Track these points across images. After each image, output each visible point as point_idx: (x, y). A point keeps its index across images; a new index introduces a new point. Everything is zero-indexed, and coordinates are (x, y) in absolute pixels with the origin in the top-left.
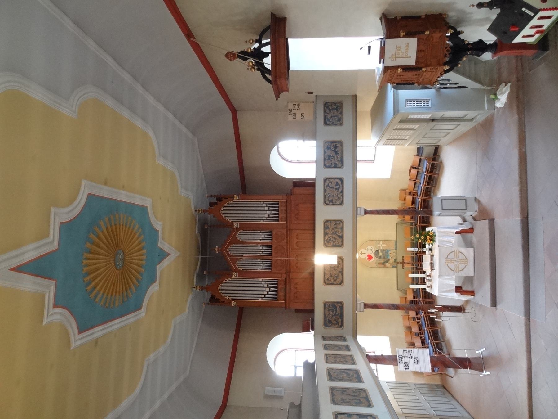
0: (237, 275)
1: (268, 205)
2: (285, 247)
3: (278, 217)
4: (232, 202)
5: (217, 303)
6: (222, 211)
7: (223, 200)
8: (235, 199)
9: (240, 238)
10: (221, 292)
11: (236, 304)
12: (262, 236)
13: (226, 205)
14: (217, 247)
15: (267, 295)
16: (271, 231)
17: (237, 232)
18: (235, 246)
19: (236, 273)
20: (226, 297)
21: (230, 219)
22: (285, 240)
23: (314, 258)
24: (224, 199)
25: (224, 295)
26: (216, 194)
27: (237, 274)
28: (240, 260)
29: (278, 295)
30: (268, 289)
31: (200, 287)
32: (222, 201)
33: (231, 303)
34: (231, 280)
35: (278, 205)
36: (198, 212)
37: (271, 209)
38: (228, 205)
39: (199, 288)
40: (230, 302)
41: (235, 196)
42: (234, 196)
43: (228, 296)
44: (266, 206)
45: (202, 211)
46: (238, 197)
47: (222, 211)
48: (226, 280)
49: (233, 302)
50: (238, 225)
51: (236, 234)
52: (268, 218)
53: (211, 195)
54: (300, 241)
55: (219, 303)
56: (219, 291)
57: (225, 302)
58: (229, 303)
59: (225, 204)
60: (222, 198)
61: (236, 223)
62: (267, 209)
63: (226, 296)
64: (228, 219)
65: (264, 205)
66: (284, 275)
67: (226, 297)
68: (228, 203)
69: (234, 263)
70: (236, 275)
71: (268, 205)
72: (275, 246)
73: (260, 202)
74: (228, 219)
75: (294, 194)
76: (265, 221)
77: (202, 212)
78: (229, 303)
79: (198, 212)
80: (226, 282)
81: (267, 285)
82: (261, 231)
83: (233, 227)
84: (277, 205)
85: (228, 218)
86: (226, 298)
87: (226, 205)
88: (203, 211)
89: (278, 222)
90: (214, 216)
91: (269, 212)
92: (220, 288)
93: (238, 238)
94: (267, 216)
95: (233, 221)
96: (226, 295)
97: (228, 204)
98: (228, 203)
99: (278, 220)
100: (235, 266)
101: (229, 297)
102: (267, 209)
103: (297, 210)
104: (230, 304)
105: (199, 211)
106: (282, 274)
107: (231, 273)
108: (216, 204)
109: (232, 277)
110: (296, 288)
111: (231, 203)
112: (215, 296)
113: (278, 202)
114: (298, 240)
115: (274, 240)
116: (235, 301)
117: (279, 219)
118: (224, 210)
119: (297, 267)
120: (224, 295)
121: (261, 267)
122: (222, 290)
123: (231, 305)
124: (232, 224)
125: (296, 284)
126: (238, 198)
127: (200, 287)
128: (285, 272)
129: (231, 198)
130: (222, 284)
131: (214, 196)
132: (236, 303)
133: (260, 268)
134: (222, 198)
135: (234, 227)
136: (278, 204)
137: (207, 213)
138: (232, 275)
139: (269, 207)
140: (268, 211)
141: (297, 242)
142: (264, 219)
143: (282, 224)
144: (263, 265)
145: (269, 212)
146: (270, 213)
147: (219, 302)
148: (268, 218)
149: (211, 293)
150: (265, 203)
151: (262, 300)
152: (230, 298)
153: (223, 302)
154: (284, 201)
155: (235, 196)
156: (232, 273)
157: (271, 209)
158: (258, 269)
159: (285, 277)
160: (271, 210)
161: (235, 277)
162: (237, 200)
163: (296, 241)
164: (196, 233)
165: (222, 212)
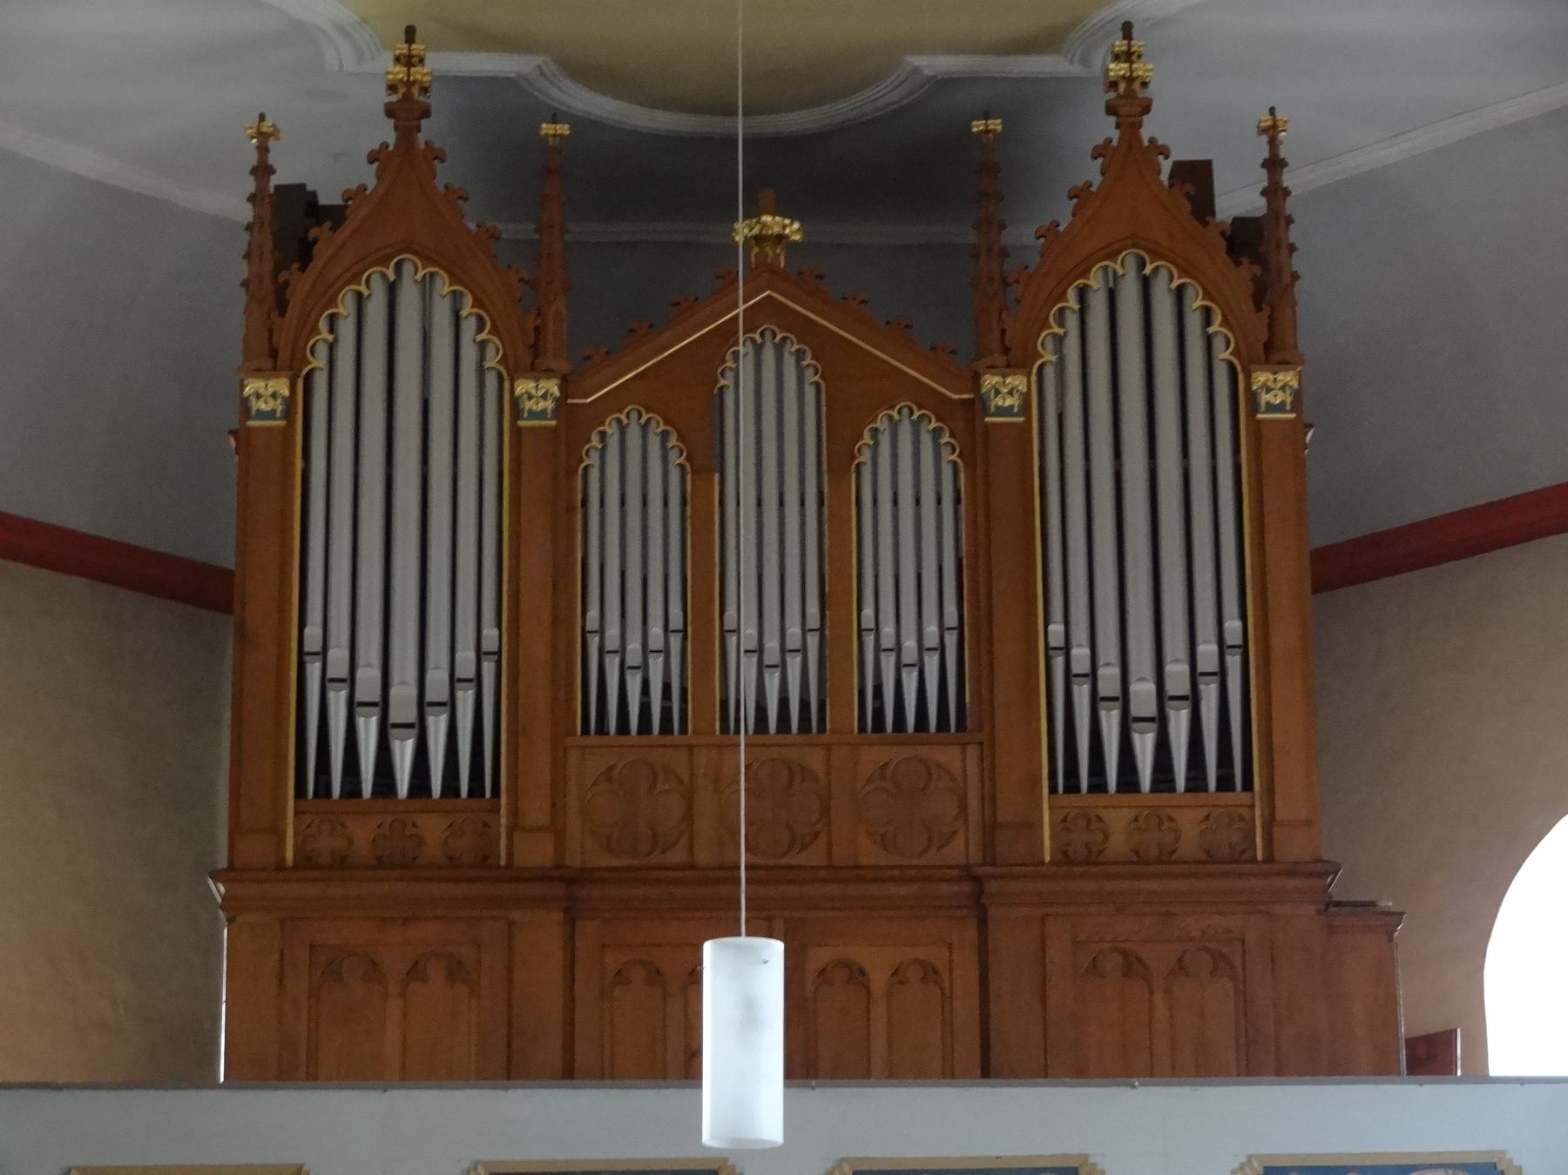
0: (534, 415)
1: (1209, 692)
2: (814, 856)
3: (1098, 785)
4: (1222, 354)
5: (269, 246)
6: (1142, 265)
7: (1247, 270)
8: (1261, 377)
9: (885, 440)
10: (377, 283)
11: (262, 415)
12: (910, 644)
13: (1195, 301)
14: (793, 229)
15: (352, 705)
16: (961, 726)
17: (942, 408)
18: (810, 392)
19: (549, 405)
20: (323, 325)
21: (1059, 340)
22: (871, 855)
23: (748, 934)
24: (1254, 279)
25: (345, 307)
26: (1290, 206)
27: (542, 415)
28: (673, 441)
29: (351, 804)
30: (403, 707)
31: (415, 90)
32: (1238, 264)
33: (274, 370)
34: (481, 371)
35: (1220, 788)
36: (1120, 45)
37: (1179, 722)
38: (1194, 322)
39: (409, 84)
40: (284, 355)
41: (1288, 377)
42: (1285, 364)
43: (332, 347)
44: (1201, 668)
45: (1130, 79)
46: (1280, 407)
47: (1142, 265)
48: (480, 329)
49: (282, 386)
50: (1007, 411)
51: (924, 397)
52: (1082, 693)
53: (1283, 164)
54: (879, 1011)
55: (267, 266)
56: (384, 261)
57: (282, 314)
58: (274, 354)
59: (1208, 295)
60: (1258, 259)
61: (1026, 398)
62: (1177, 673)
63: (332, 330)
64: (1061, 324)
65: (1213, 648)
66: (536, 852)
67: (323, 325)
68: (1218, 318)
69: (647, 394)
70: (529, 405)
71: (1209, 692)
72: (815, 760)
73: (1243, 617)
74: (1061, 324)
75: (1331, 930)
76: (1059, 662)
77: (1122, 87)
78: (274, 354)
79: (1120, 45)
80: (469, 327)
81: (444, 696)
82: (960, 628)
83: (992, 368)
84: (1219, 779)
85: (1072, 321)
86: (315, 330)
87: (1199, 303)
88: (1130, 95)
89: (1053, 789)
90: (1081, 195)
91: (1143, 692)
92: (407, 269)
93: (882, 424)
94: (1109, 676)
95: (1050, 373)
96: (347, 328)
97: (1208, 322)
98: (1218, 318)
99: (1072, 787)
100: (614, 402)
101: (322, 351)
102: (1177, 673)
103: (1181, 967)
104: (268, 363)
105: (1128, 56)
106: (557, 829)
107: (554, 365)
108: (1203, 204)
109: (514, 368)
110: (416, 972)
111: (1218, 343)
112: (334, 229)
113: (1248, 785)
114: (879, 980)
115: (873, 756)
116: (289, 403)
117: (1084, 798)
118: (1146, 284)
119: (621, 977)
120: (341, 310)
121: (612, 641)
122: (392, 290)
123: (258, 372)
124: (1018, 359)
125: (457, 971)
126: (1271, 408)
127: (415, 90)
128: (574, 860)
129: (1269, 347)
130: (443, 286)
131: (1275, 192)
132: (270, 415)
133: (601, 631)
134: (1258, 259)
135: (990, 381)
136: (1225, 783)
137: (1107, 129)
138: (535, 370)
139: (1194, 699)
140: (1150, 687)
141: (857, 975)
142: (1075, 652)
143: (1033, 826)
144: (634, 657)
145: (1143, 692)
146: (1135, 710)
147: (278, 268)
148: (1082, 693)
149: (363, 188)
150: (1234, 662)
151: (301, 653)
152: (319, 361)
153: (282, 306)
154: (1259, 840)
155: (1280, 376)
156: (549, 373)
157: (1179, 722)
158: (593, 613)
159: (519, 860)
160: (1161, 722)
161: (516, 403)
162: (1253, 398)
163: (878, 962)
164: (918, 61)
165: (1126, 267)
